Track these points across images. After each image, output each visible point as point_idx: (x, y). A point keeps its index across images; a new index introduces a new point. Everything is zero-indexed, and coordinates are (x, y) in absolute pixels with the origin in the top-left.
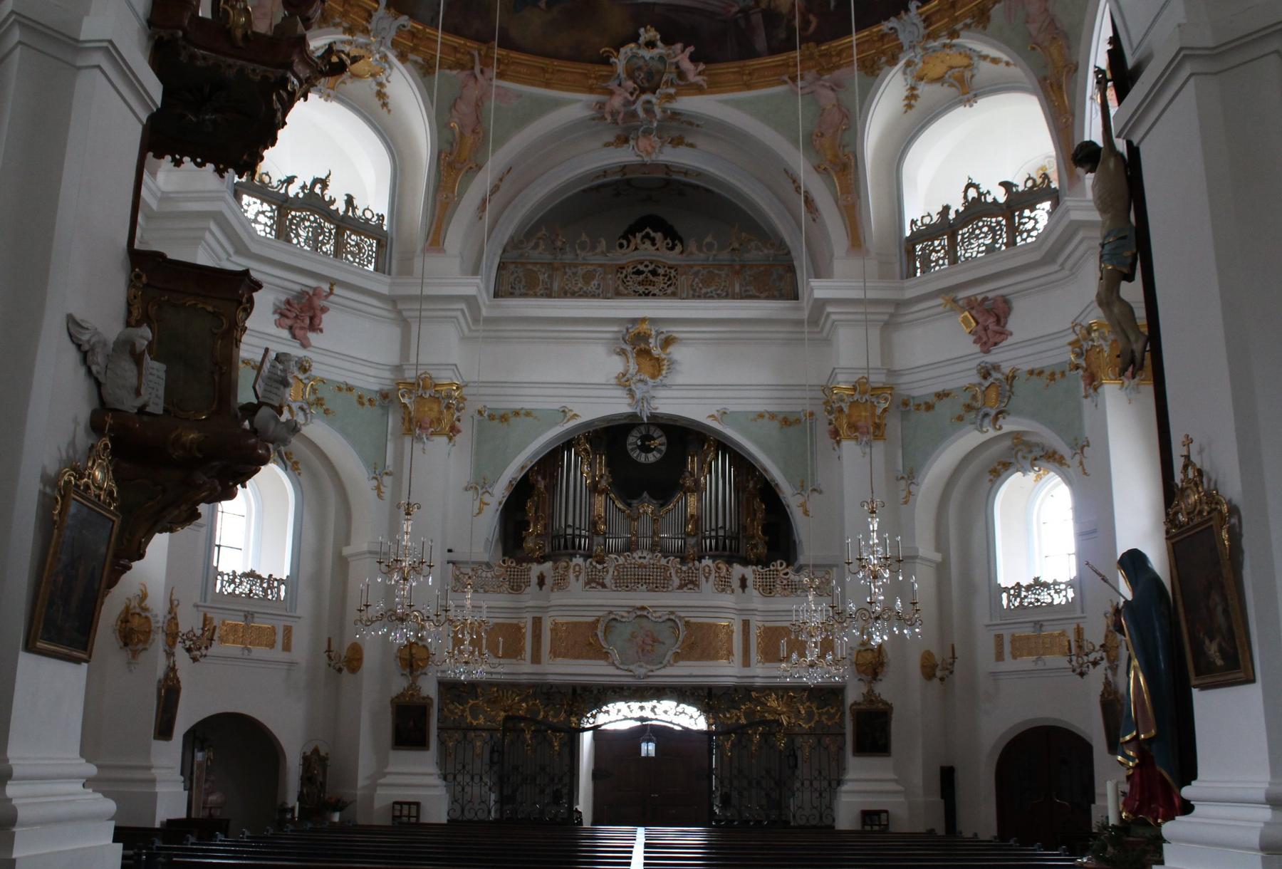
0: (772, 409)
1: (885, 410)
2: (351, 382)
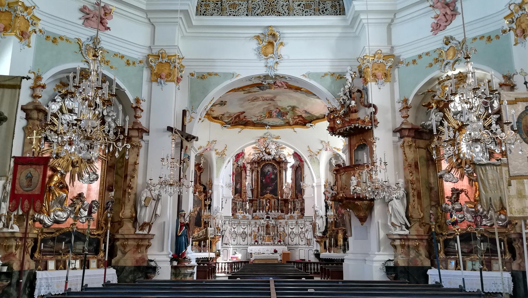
0: (332, 71)
1: (390, 67)
2: (122, 53)
